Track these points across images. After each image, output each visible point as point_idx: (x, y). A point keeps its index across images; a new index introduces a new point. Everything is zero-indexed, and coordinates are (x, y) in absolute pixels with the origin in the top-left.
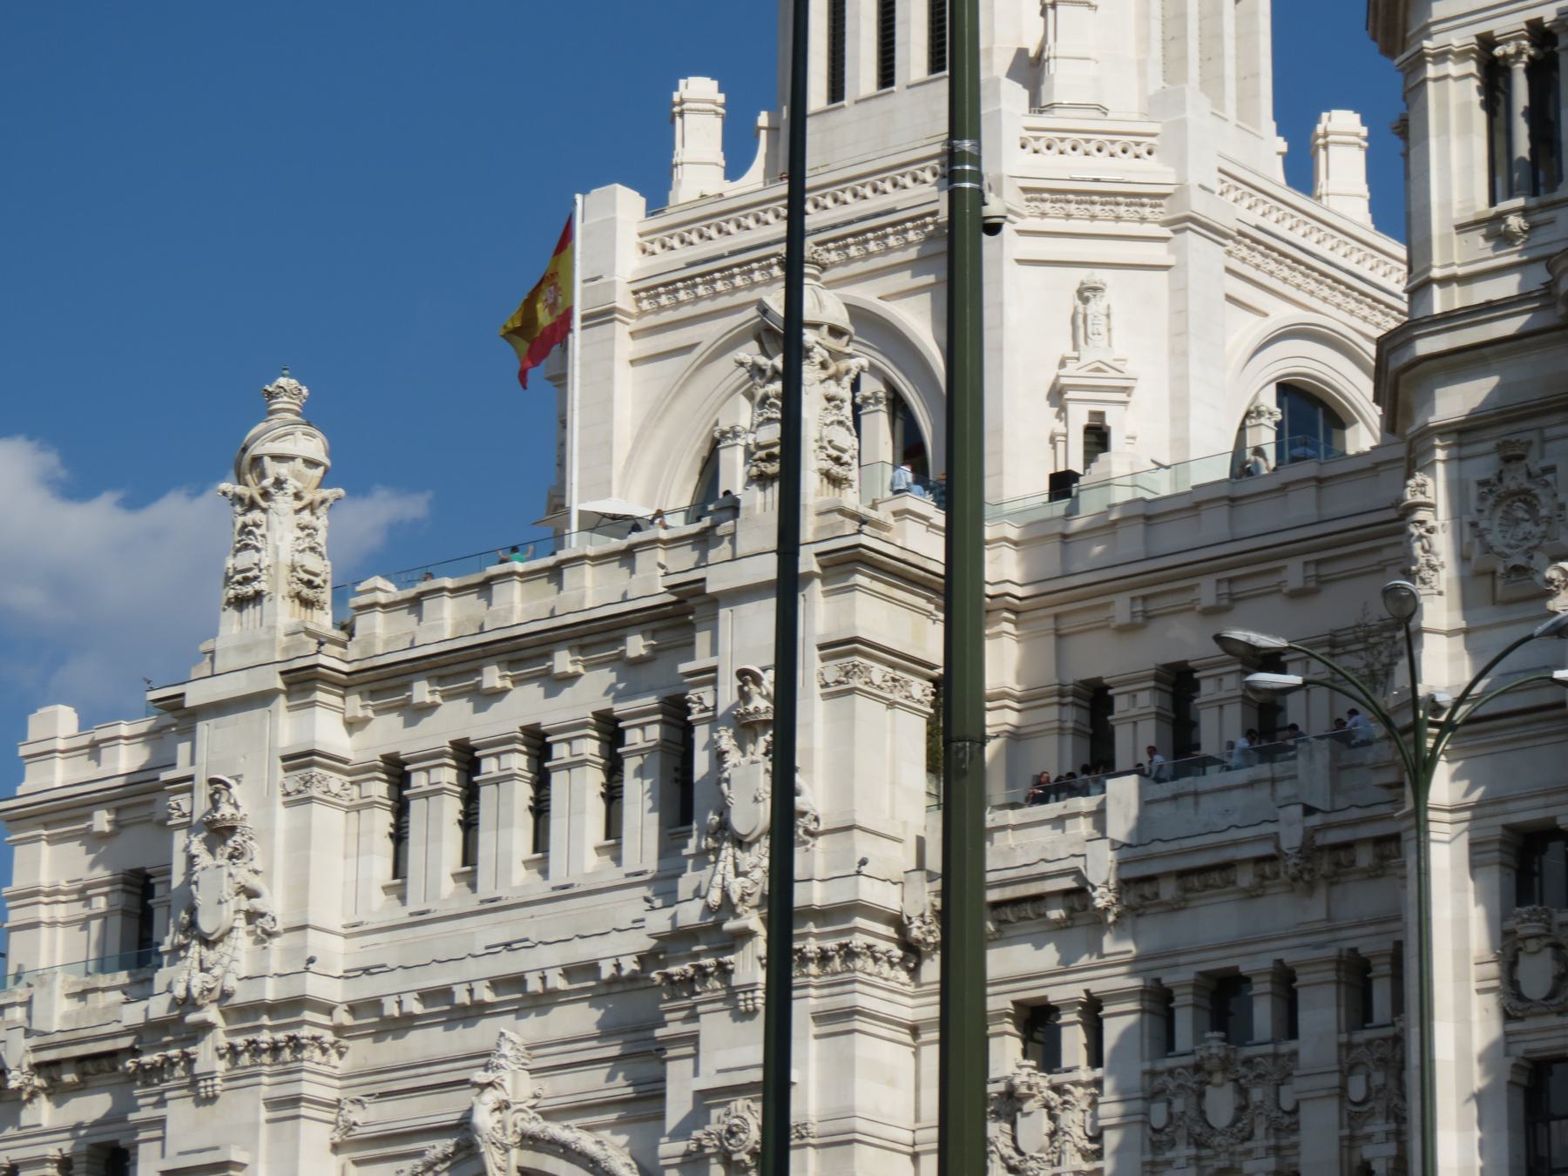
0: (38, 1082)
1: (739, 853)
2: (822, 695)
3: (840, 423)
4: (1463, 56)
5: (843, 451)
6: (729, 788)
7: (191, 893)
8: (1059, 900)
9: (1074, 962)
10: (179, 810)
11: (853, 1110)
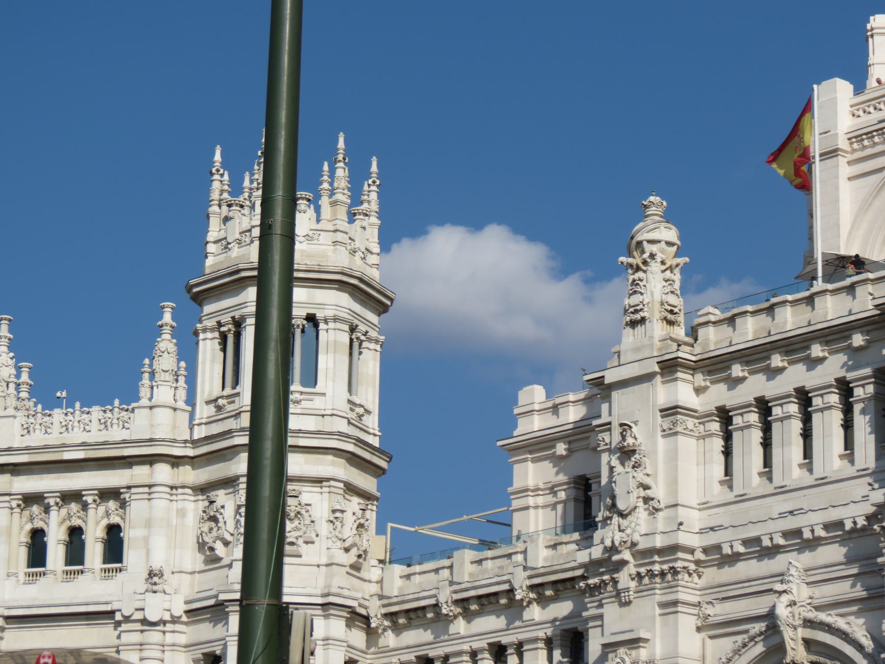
0: (387, 623)
1: (621, 519)
2: (662, 436)
3: (672, 292)
4: (212, 330)
5: (675, 307)
6: (616, 486)
7: (612, 487)
8: (550, 586)
9: (512, 624)
10: (604, 441)
11: (678, 654)
